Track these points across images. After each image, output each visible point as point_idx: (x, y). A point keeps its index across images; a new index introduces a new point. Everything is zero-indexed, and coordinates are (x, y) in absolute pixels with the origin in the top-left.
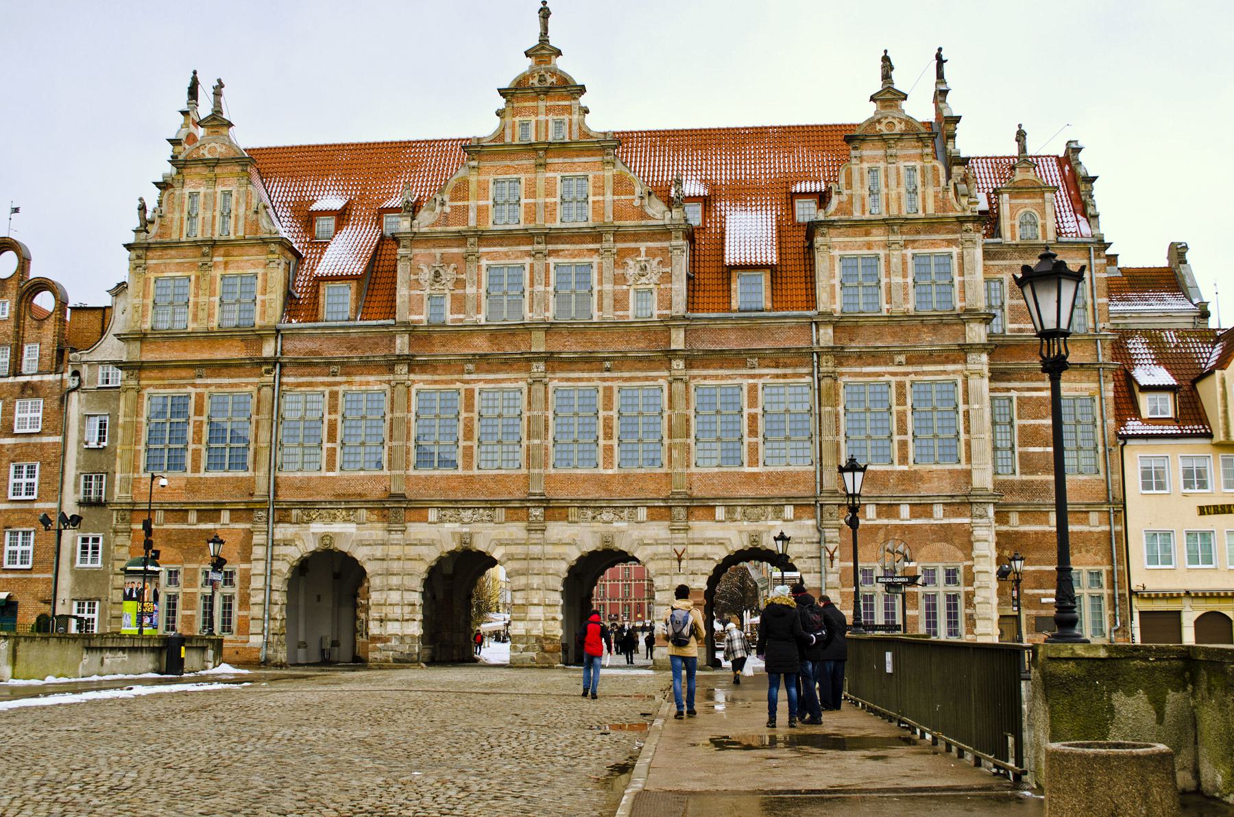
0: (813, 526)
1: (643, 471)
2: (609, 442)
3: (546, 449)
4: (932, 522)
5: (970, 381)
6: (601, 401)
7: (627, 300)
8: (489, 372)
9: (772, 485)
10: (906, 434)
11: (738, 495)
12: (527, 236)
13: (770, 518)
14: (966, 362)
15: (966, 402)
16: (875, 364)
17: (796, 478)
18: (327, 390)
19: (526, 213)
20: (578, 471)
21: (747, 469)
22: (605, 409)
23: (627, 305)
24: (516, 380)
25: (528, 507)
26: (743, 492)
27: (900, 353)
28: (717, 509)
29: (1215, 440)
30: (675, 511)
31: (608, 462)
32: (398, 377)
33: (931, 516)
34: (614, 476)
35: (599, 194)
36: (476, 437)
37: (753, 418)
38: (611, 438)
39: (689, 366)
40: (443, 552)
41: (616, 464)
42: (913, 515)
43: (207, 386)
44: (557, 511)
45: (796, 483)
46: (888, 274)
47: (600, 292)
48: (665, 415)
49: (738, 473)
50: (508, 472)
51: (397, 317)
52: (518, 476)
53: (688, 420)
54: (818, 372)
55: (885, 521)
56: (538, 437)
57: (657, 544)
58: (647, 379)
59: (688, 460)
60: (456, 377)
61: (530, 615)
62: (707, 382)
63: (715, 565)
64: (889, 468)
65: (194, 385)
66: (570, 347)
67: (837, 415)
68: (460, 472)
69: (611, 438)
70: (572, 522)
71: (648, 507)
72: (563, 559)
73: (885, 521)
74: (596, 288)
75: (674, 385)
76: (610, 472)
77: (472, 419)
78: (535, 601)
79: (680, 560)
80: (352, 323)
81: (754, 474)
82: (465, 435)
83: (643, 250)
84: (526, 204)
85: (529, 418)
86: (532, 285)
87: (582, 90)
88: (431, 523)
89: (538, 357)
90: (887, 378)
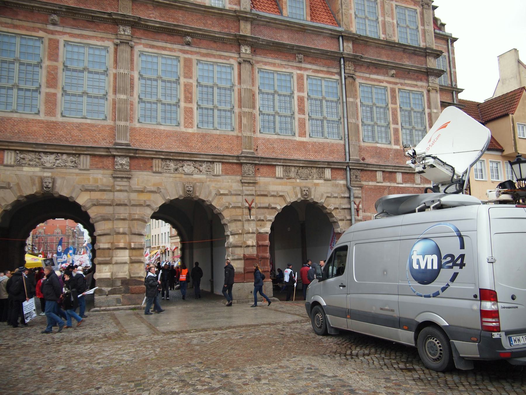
0: (344, 185)
1: (218, 132)
2: (189, 105)
3: (132, 104)
5: (431, 94)
6: (182, 69)
8: (74, 27)
9: (316, 152)
10: (397, 124)
11: (292, 158)
13: (315, 177)
14: (428, 81)
15: (429, 108)
16: (378, 74)
17: (332, 149)
20: (162, 128)
21: (297, 138)
22: (185, 77)
24: (102, 39)
25: (114, 156)
26: (296, 156)
27: (393, 68)
28: (277, 168)
29: (505, 153)
30: (246, 168)
31: (189, 122)
33: (413, 182)
34: (193, 134)
36: (60, 85)
37: (301, 100)
38: (191, 102)
39: (254, 51)
40: (21, 196)
41: (195, 124)
42: (404, 181)
44: (141, 162)
45: (332, 152)
46: (383, 15)
48: (236, 89)
49: (291, 141)
50: (93, 122)
52: (104, 127)
53: (253, 95)
54: (345, 73)
55: (388, 184)
56: (125, 93)
57: (232, 195)
58: (220, 57)
60: (39, 25)
61: (115, 259)
62: (267, 67)
63: (277, 213)
64: (389, 146)
68: (42, 117)
69: (191, 102)
70: (154, 172)
71: (223, 163)
72: (148, 206)
73: (388, 184)
75: (243, 65)
76: (190, 130)
77: (56, 68)
78: (122, 245)
79: (250, 209)
81: (303, 142)
82: (48, 82)
85: (115, 75)
89: (124, 21)
90: (385, 84)
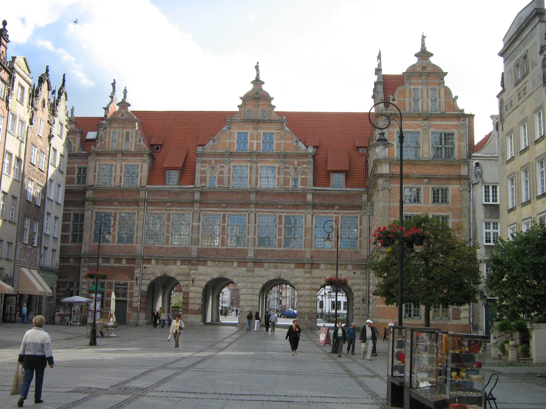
12: (250, 155)
23: (289, 184)
47: (278, 178)
66: (266, 198)
74: (277, 176)
76: (280, 249)
80: (178, 186)
87: (272, 99)
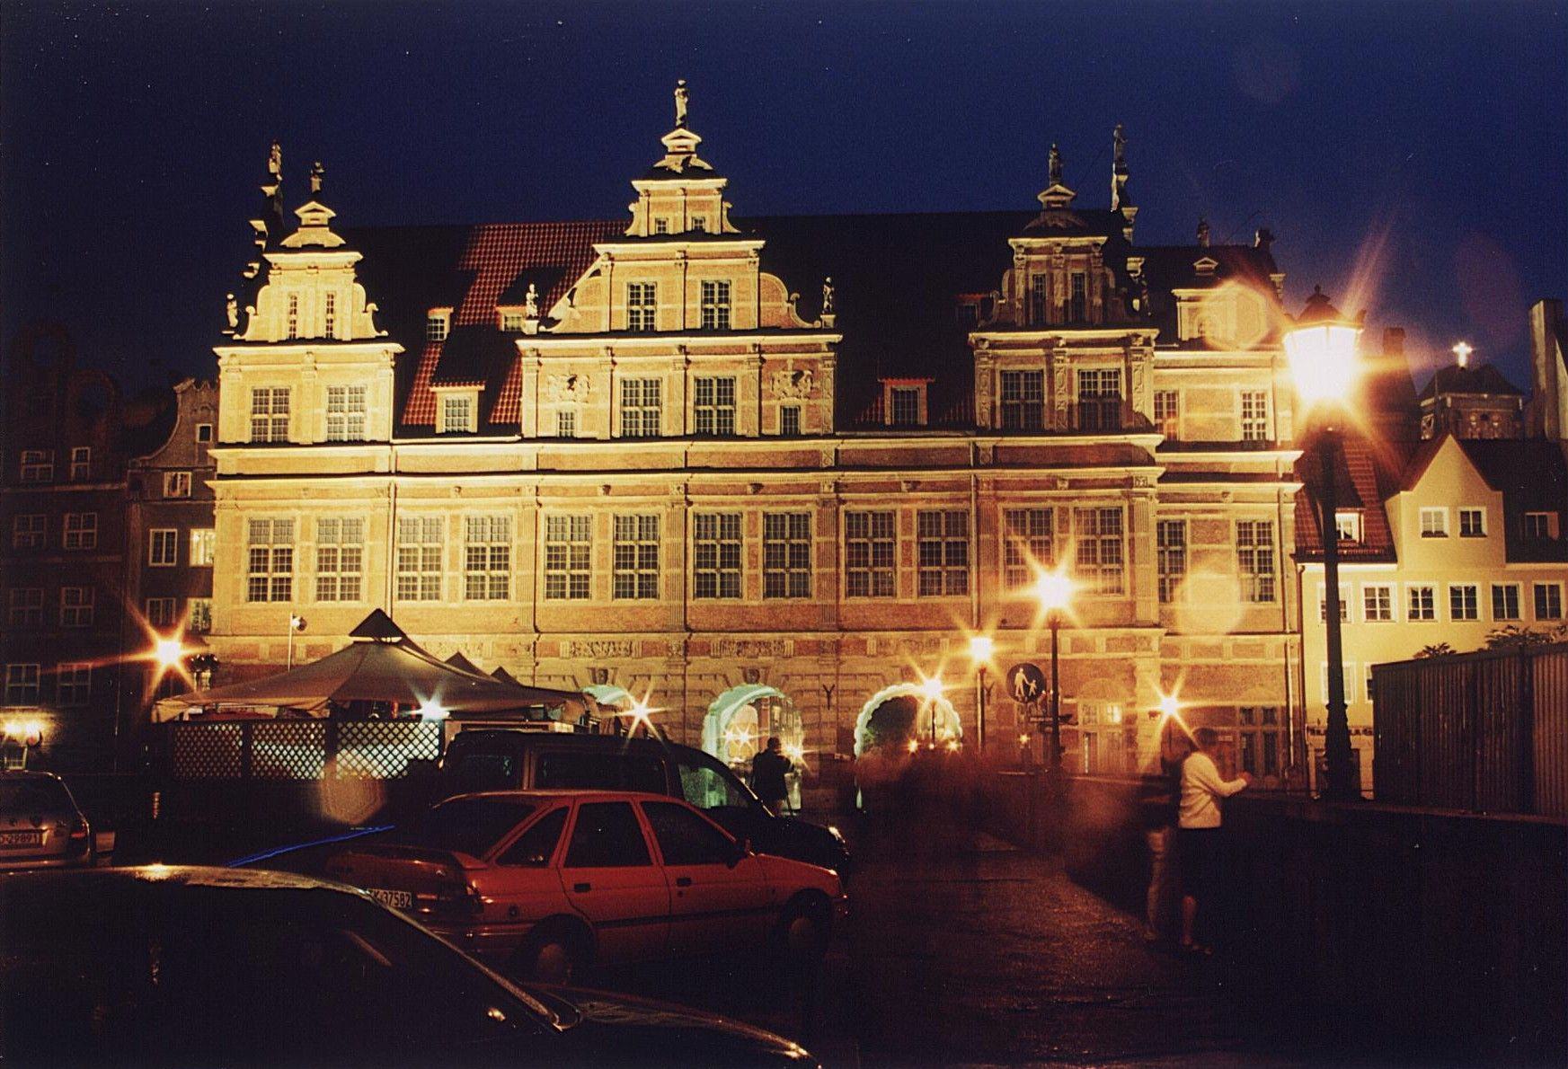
4: (1093, 656)
7: (774, 417)
18: (448, 514)
19: (664, 319)
21: (901, 601)
24: (654, 504)
32: (526, 499)
34: (759, 607)
35: (743, 300)
43: (313, 508)
49: (891, 605)
51: (523, 432)
53: (838, 547)
56: (679, 566)
58: (794, 503)
59: (838, 591)
65: (299, 507)
67: (996, 543)
70: (714, 657)
76: (755, 603)
81: (909, 605)
83: (790, 363)
84: (663, 310)
85: (667, 545)
86: (670, 398)
88: (563, 658)
90: (1049, 503)
